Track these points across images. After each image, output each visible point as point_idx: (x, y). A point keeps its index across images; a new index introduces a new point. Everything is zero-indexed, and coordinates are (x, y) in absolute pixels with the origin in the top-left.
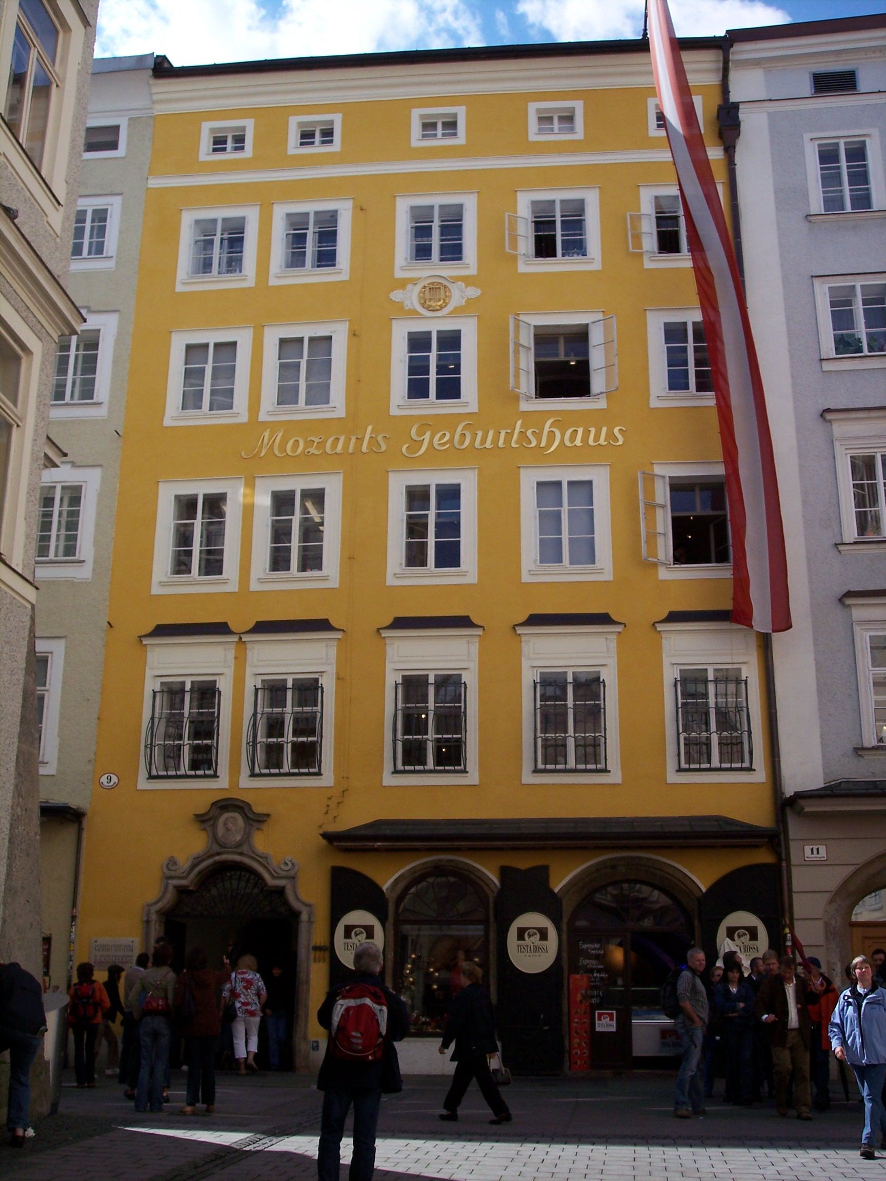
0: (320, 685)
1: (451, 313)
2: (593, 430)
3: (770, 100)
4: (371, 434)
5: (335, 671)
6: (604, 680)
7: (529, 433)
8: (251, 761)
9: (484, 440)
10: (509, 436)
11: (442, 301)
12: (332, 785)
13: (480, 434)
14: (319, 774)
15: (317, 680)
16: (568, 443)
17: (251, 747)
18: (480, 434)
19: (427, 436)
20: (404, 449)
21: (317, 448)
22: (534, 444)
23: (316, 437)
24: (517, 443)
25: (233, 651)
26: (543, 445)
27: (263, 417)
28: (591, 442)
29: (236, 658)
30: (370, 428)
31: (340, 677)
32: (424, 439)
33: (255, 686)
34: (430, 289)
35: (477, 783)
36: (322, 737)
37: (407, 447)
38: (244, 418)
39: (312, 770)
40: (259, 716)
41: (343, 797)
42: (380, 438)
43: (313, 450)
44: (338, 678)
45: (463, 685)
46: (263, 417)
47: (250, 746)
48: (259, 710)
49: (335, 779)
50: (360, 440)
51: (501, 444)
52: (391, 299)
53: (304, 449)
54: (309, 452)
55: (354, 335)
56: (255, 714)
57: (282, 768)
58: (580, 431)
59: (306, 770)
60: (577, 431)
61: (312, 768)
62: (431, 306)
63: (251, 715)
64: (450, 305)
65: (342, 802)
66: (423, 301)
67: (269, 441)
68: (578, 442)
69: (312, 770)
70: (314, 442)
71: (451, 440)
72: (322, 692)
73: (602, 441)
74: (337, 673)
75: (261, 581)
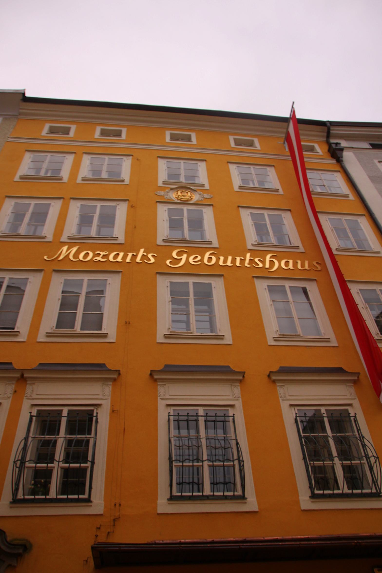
0: (95, 414)
1: (195, 202)
2: (299, 262)
3: (353, 148)
4: (144, 252)
5: (109, 404)
6: (355, 414)
7: (256, 260)
8: (15, 484)
9: (225, 261)
10: (242, 261)
11: (189, 198)
12: (102, 512)
13: (222, 258)
14: (88, 500)
15: (90, 413)
16: (283, 266)
17: (17, 469)
18: (222, 258)
19: (184, 257)
20: (168, 262)
21: (102, 258)
22: (261, 265)
23: (102, 252)
24: (249, 264)
25: (13, 386)
26: (267, 266)
27: (64, 239)
28: (299, 267)
29: (15, 392)
30: (142, 250)
31: (114, 409)
32: (181, 259)
33: (31, 413)
34: (181, 192)
35: (257, 510)
36: (93, 463)
37: (170, 262)
38: (50, 238)
39: (81, 496)
40: (30, 439)
41: (114, 525)
42: (150, 256)
43: (99, 259)
44: (113, 411)
45: (231, 419)
46: (64, 239)
47: (17, 467)
48: (31, 435)
49: (105, 506)
50: (135, 257)
51: (238, 264)
52: (156, 194)
53: (94, 257)
54: (96, 259)
55: (132, 206)
56: (26, 439)
57: (48, 495)
58: (291, 262)
59: (76, 497)
60: (288, 262)
61: (81, 494)
62: (181, 198)
63: (23, 438)
64: (193, 200)
65: (113, 532)
66: (177, 196)
67: (67, 251)
68: (291, 266)
69: (81, 496)
70: (100, 254)
71: (202, 260)
72: (97, 422)
73: (307, 267)
74: (112, 406)
75: (49, 335)
